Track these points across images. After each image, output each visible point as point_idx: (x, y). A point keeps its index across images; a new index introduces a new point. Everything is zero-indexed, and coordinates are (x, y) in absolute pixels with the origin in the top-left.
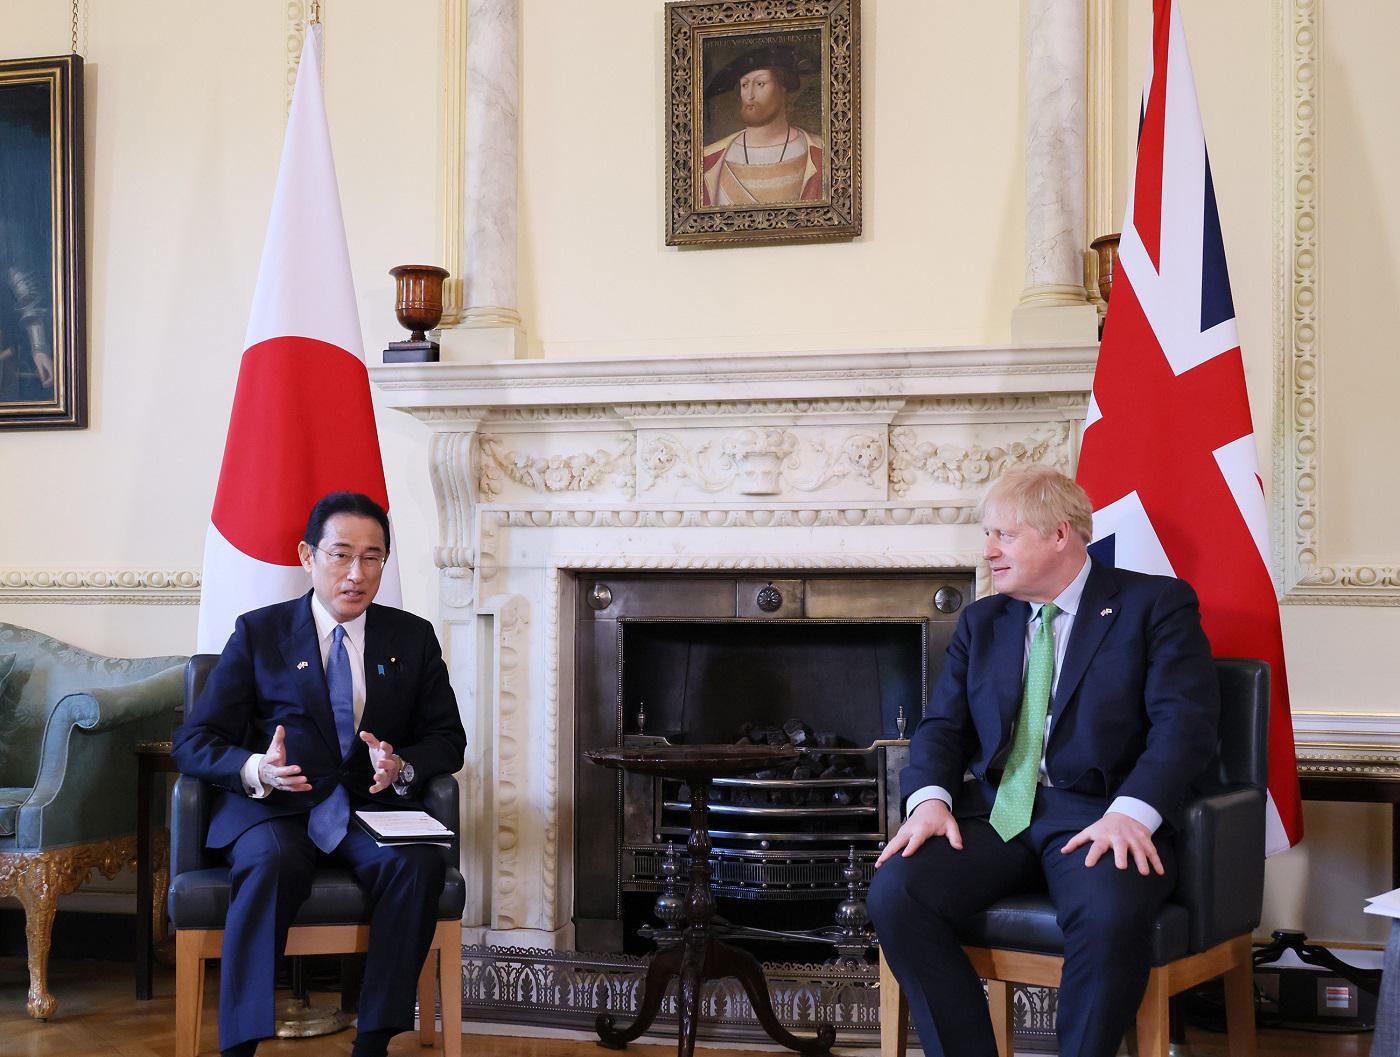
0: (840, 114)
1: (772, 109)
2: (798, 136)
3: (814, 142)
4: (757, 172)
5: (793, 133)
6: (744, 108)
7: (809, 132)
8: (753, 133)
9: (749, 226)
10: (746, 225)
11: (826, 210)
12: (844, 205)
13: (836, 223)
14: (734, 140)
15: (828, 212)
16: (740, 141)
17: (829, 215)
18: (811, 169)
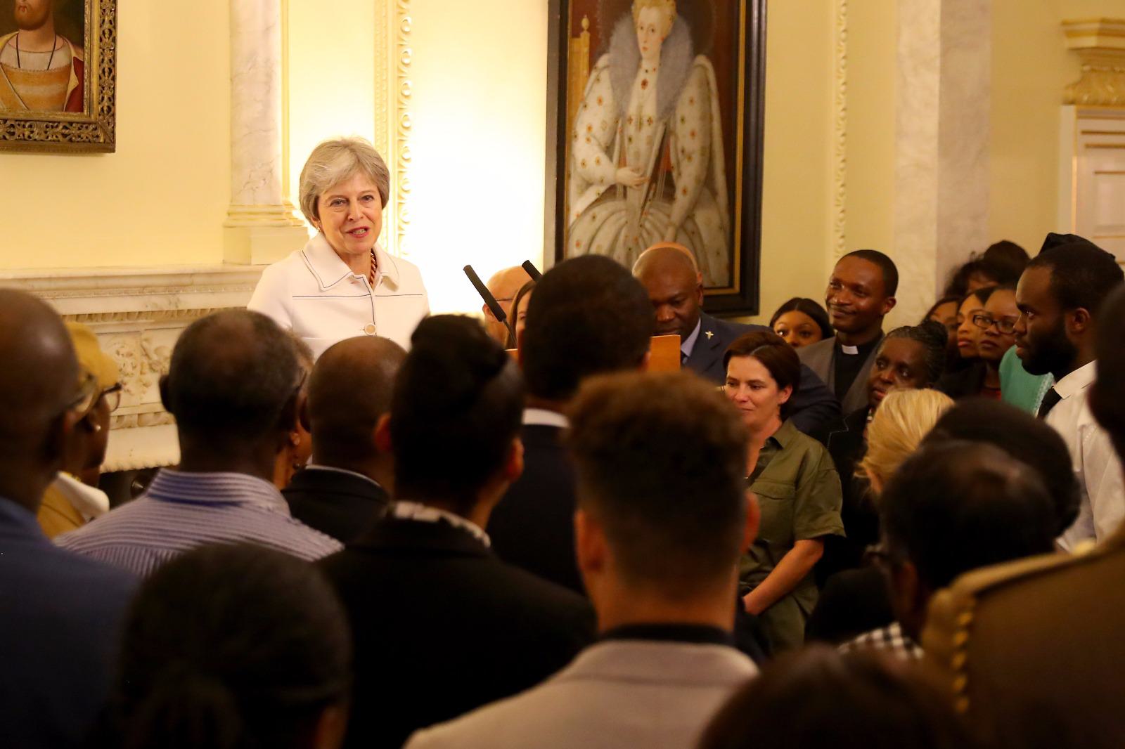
0: (107, 32)
1: (40, 15)
2: (63, 46)
3: (77, 53)
4: (29, 78)
5: (60, 41)
6: (17, 9)
7: (72, 43)
8: (26, 36)
9: (29, 137)
10: (27, 133)
11: (91, 127)
12: (109, 123)
13: (102, 140)
14: (8, 41)
15: (95, 129)
16: (13, 42)
17: (99, 132)
18: (73, 82)
